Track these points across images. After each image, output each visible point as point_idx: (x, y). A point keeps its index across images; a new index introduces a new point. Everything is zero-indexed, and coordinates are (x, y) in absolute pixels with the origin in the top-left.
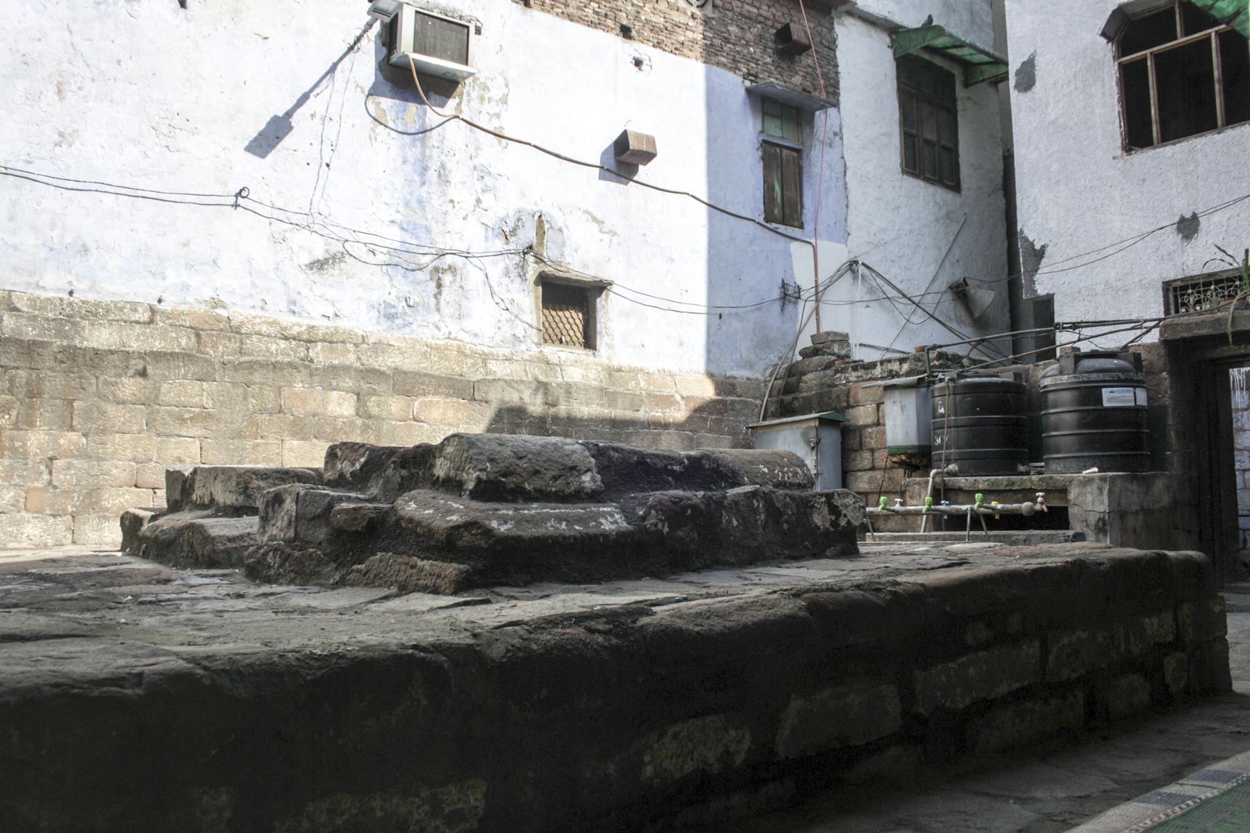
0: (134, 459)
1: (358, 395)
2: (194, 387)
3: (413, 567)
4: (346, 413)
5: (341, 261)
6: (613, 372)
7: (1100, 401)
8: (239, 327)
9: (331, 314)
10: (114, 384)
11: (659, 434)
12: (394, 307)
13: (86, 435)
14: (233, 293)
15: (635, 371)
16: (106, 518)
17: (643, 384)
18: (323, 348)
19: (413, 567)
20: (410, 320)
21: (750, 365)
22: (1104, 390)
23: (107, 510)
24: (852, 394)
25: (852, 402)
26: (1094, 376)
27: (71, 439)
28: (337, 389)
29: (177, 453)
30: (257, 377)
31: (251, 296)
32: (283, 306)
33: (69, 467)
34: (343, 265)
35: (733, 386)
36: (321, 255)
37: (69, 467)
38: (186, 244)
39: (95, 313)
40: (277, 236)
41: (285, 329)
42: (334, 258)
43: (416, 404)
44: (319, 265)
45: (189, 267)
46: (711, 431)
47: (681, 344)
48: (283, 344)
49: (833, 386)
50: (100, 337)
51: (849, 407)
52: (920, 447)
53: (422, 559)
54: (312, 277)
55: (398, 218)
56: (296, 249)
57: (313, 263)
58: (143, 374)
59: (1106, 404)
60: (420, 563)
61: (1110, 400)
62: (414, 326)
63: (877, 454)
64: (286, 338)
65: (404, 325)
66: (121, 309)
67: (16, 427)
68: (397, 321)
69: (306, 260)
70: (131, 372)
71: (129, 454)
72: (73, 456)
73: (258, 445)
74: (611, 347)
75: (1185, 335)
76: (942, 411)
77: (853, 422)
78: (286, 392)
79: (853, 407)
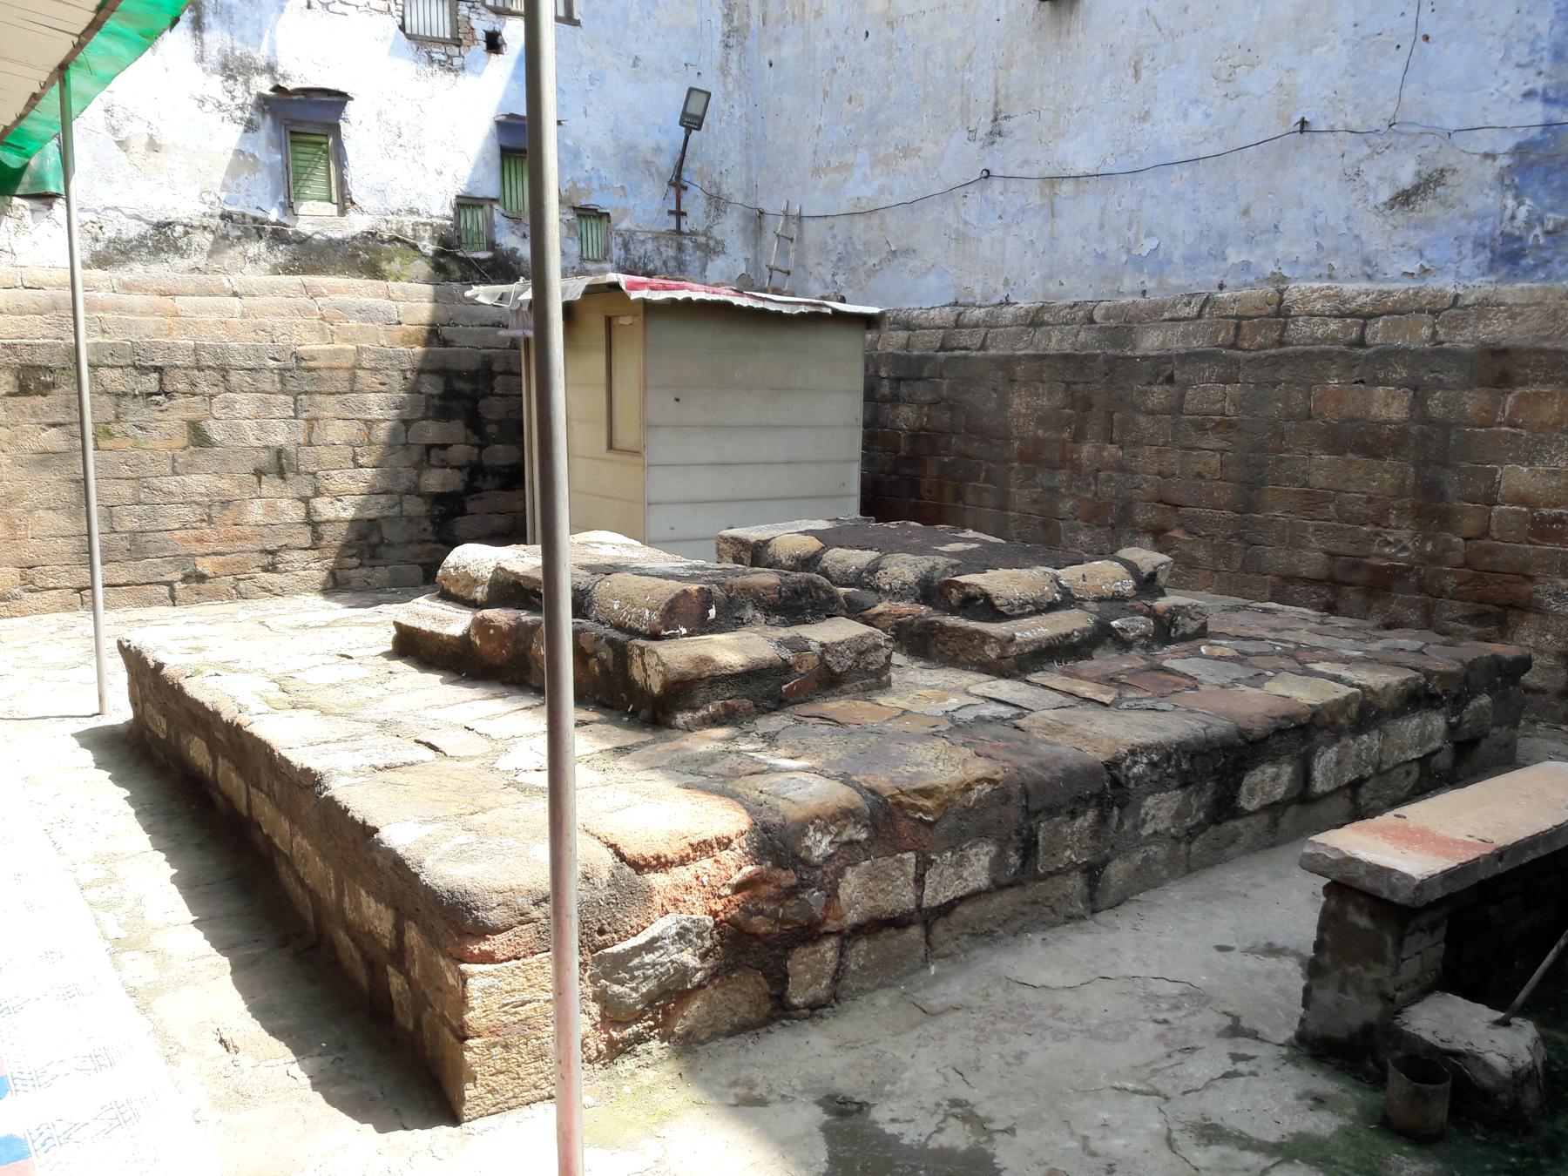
0: (1159, 474)
1: (1416, 390)
2: (1215, 390)
4: (1395, 417)
5: (1438, 183)
8: (1288, 309)
9: (1413, 267)
10: (1145, 393)
12: (1520, 239)
13: (1121, 448)
14: (1297, 261)
16: (1137, 533)
18: (1386, 322)
20: (1546, 254)
23: (1137, 524)
27: (1112, 450)
28: (1385, 383)
29: (1199, 467)
30: (1283, 375)
31: (1316, 263)
32: (1356, 267)
33: (1110, 479)
34: (1439, 190)
36: (1406, 179)
37: (1110, 479)
38: (1246, 212)
39: (1156, 314)
40: (1349, 171)
41: (1344, 302)
42: (1427, 182)
43: (1510, 398)
44: (1404, 199)
45: (1250, 240)
48: (1334, 325)
50: (1151, 342)
54: (1391, 221)
55: (1539, 84)
56: (1373, 182)
57: (1394, 199)
58: (1170, 380)
62: (1556, 265)
64: (1342, 316)
65: (1535, 267)
66: (1174, 305)
67: (1075, 441)
68: (1523, 262)
69: (1385, 195)
70: (1161, 379)
71: (1156, 468)
72: (1112, 469)
73: (1282, 460)
78: (1317, 390)
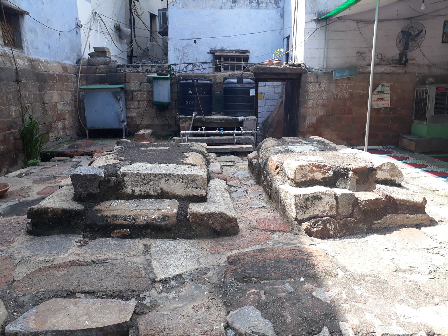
3: (407, 218)
6: (31, 61)
7: (249, 93)
11: (52, 93)
15: (38, 61)
17: (42, 68)
19: (407, 218)
21: (68, 58)
24: (127, 77)
25: (127, 80)
26: (248, 86)
35: (66, 68)
46: (65, 90)
47: (49, 47)
49: (117, 72)
51: (126, 82)
52: (169, 103)
53: (411, 215)
60: (410, 216)
63: (140, 102)
74: (28, 48)
75: (261, 72)
76: (191, 92)
77: (128, 89)
79: (128, 83)
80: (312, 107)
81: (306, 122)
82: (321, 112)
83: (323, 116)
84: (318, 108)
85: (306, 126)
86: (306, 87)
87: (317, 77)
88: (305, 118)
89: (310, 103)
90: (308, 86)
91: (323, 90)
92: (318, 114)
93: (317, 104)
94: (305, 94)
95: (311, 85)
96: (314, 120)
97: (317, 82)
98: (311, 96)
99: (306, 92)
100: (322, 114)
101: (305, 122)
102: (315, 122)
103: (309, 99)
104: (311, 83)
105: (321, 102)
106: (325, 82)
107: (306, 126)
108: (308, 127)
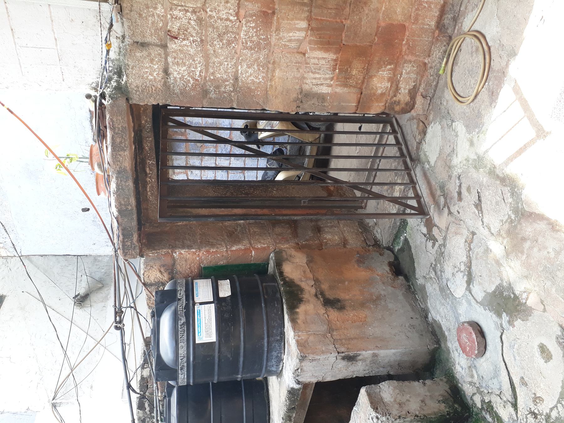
22: (197, 342)
59: (213, 338)
61: (209, 335)
80: (269, 66)
81: (325, 90)
82: (294, 30)
83: (309, 19)
84: (273, 40)
85: (339, 90)
86: (183, 92)
87: (143, 45)
88: (307, 95)
89: (250, 75)
90: (180, 83)
91: (200, 21)
92: (300, 42)
93: (257, 47)
94: (212, 95)
95: (177, 72)
96: (322, 59)
97: (164, 46)
98: (223, 70)
99: (205, 93)
100: (303, 24)
101: (322, 97)
102: (331, 56)
103: (236, 79)
104: (166, 72)
105: (248, 31)
106: (160, 10)
107: (339, 90)
108: (345, 85)
